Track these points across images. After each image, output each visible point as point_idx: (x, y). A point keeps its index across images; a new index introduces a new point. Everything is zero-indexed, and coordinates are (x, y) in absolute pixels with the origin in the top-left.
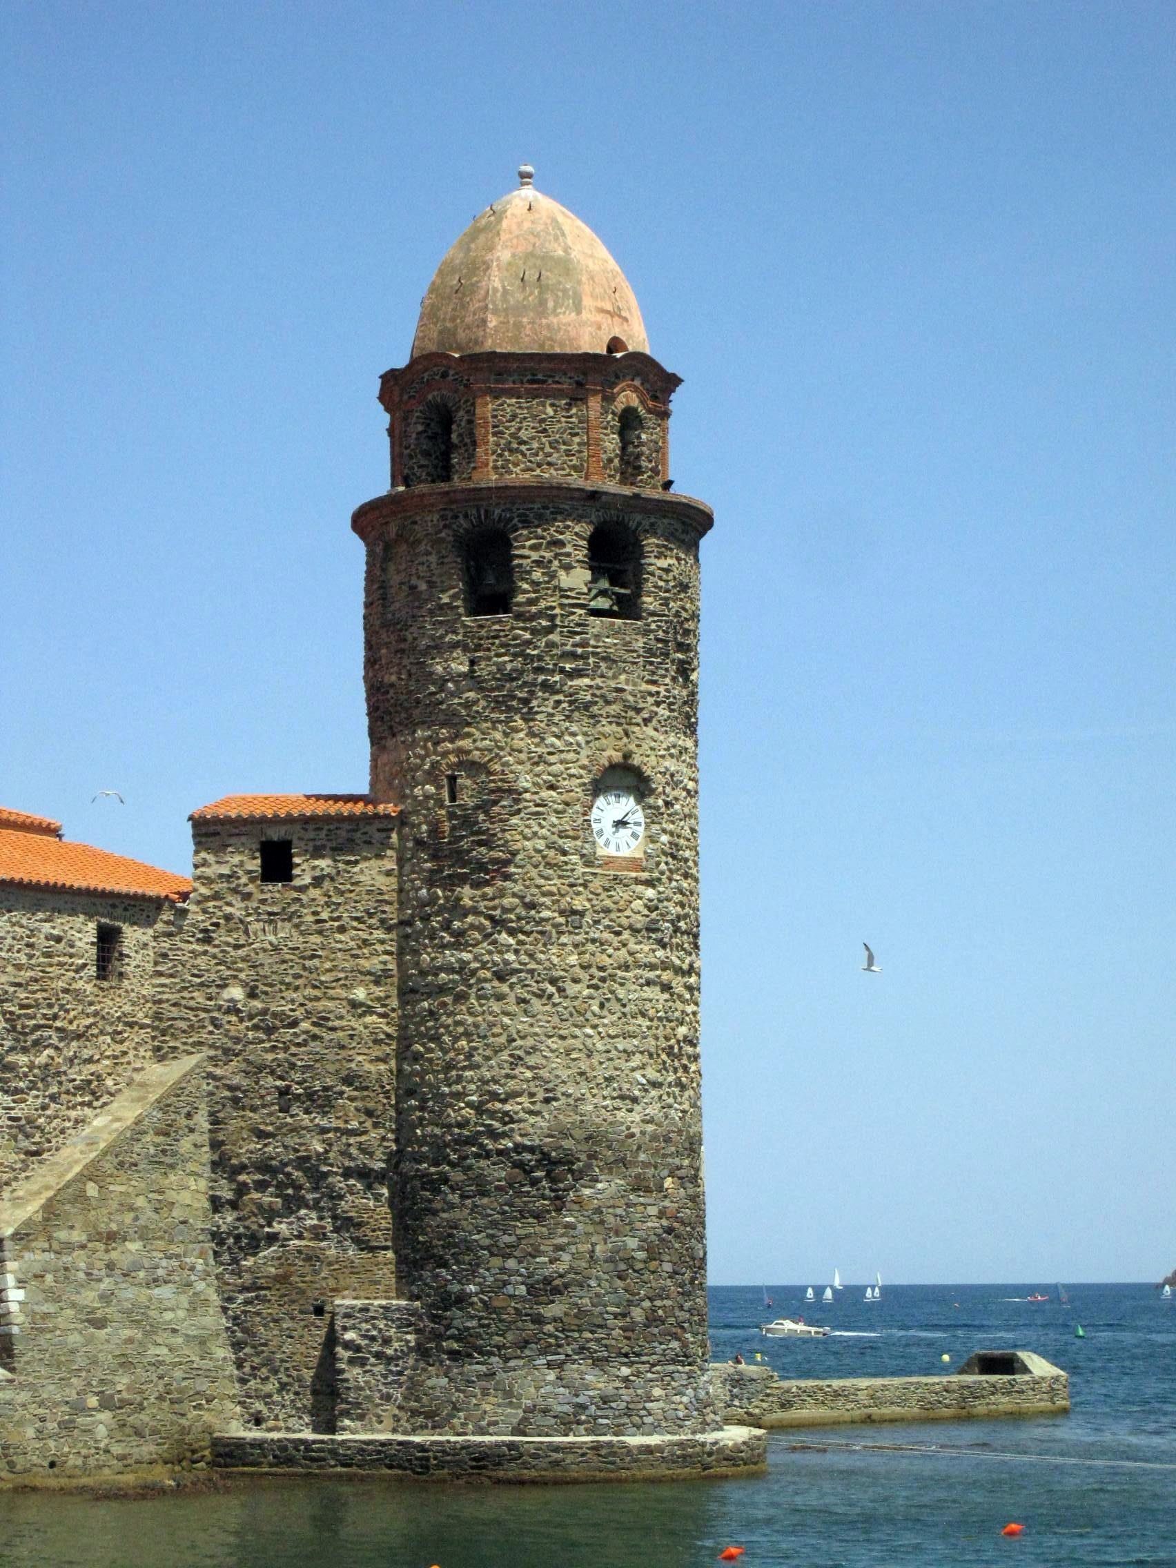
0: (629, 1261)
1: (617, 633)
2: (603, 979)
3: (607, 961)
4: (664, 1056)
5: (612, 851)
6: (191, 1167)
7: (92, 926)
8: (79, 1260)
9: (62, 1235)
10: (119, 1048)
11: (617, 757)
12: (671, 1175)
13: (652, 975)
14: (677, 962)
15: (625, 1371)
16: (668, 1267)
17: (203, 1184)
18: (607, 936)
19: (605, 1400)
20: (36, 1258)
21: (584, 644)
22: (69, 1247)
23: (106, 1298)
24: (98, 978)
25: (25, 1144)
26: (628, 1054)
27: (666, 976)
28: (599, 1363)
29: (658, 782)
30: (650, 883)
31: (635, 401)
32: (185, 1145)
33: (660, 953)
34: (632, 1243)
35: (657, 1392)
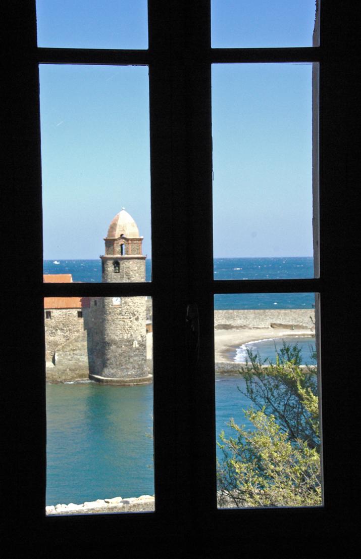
0: (116, 356)
2: (113, 320)
7: (76, 312)
8: (68, 353)
9: (65, 350)
16: (123, 357)
20: (61, 353)
22: (66, 351)
23: (72, 357)
26: (117, 330)
27: (123, 320)
28: (112, 369)
30: (120, 308)
31: (123, 243)
33: (122, 317)
35: (120, 373)
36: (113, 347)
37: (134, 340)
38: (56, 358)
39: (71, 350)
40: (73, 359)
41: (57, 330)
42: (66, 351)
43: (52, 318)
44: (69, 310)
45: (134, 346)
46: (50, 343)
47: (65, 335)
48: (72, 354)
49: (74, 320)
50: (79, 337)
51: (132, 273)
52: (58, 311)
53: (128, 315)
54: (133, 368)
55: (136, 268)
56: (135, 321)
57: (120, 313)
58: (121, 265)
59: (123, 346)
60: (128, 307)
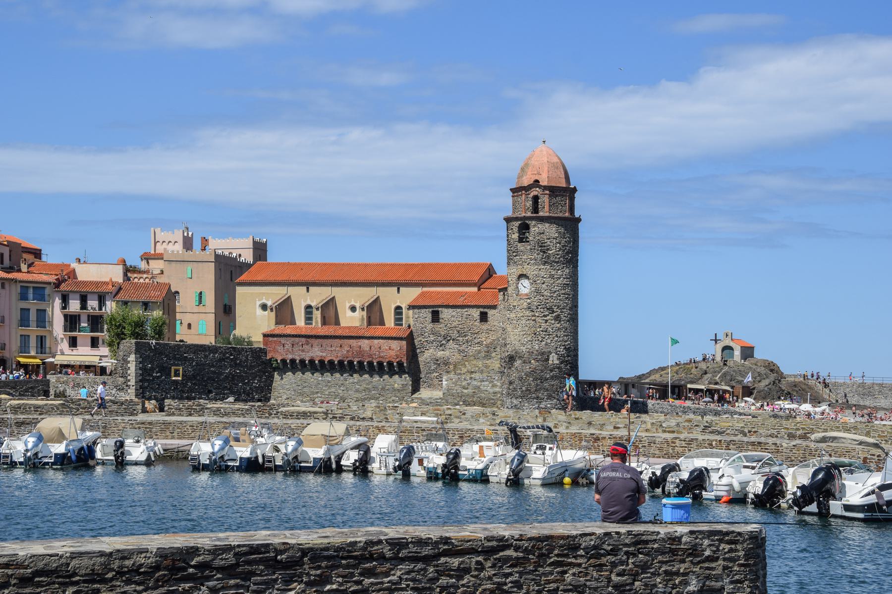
0: (522, 378)
1: (524, 246)
3: (518, 315)
4: (533, 335)
5: (523, 292)
6: (495, 359)
9: (459, 372)
10: (487, 335)
11: (521, 273)
12: (534, 360)
13: (530, 318)
14: (537, 315)
15: (521, 400)
16: (531, 379)
17: (498, 362)
18: (519, 311)
19: (516, 406)
20: (452, 375)
21: (517, 249)
22: (460, 374)
23: (469, 384)
24: (481, 322)
25: (462, 354)
29: (531, 276)
32: (493, 354)
34: (523, 374)
36: (518, 363)
37: (550, 353)
38: (444, 383)
39: (468, 371)
40: (470, 387)
41: (449, 340)
42: (460, 374)
43: (440, 321)
44: (467, 309)
45: (550, 362)
46: (437, 360)
47: (461, 348)
48: (468, 378)
49: (475, 326)
50: (479, 352)
51: (549, 243)
52: (450, 310)
53: (542, 310)
54: (547, 399)
55: (557, 235)
56: (553, 322)
57: (529, 308)
58: (532, 229)
59: (533, 361)
60: (542, 298)
